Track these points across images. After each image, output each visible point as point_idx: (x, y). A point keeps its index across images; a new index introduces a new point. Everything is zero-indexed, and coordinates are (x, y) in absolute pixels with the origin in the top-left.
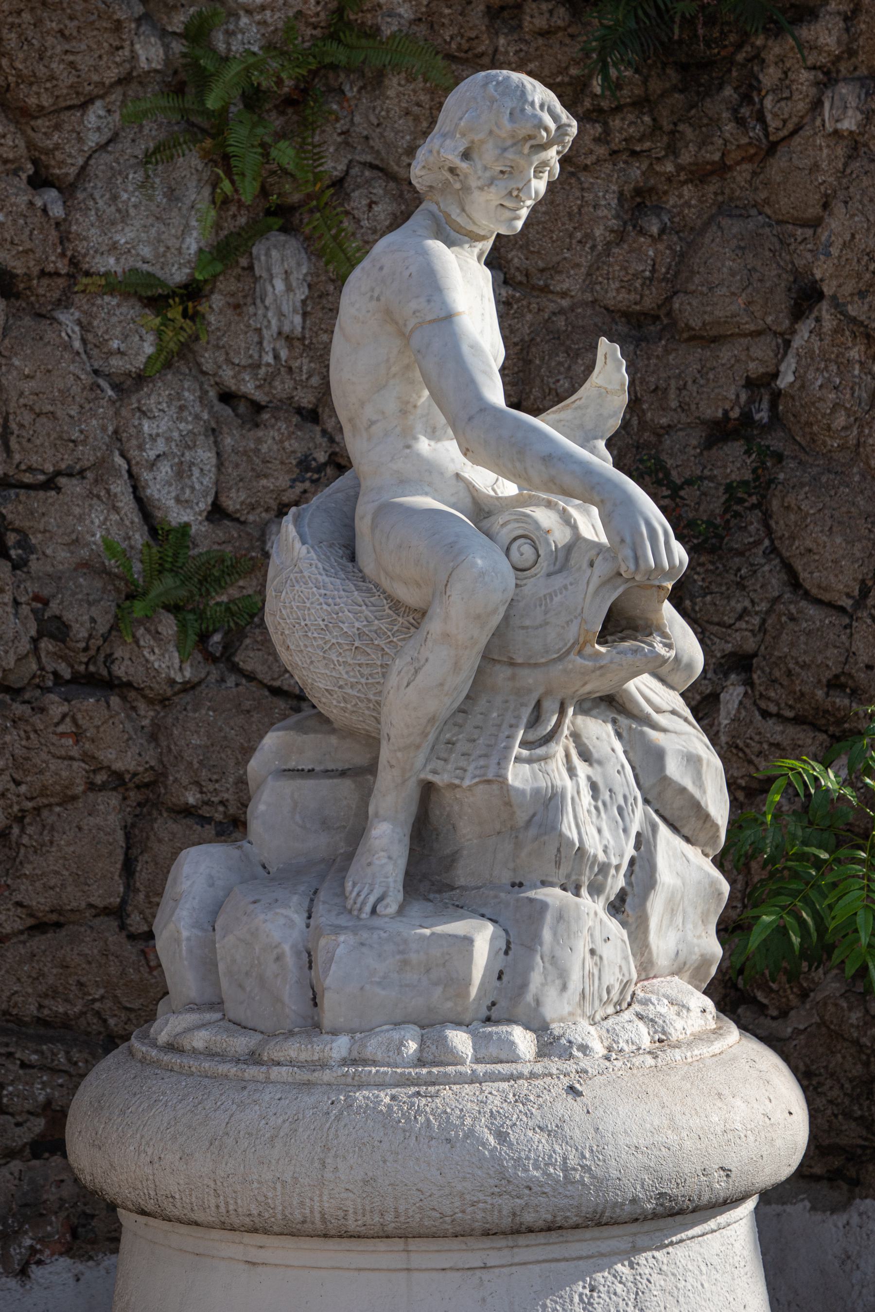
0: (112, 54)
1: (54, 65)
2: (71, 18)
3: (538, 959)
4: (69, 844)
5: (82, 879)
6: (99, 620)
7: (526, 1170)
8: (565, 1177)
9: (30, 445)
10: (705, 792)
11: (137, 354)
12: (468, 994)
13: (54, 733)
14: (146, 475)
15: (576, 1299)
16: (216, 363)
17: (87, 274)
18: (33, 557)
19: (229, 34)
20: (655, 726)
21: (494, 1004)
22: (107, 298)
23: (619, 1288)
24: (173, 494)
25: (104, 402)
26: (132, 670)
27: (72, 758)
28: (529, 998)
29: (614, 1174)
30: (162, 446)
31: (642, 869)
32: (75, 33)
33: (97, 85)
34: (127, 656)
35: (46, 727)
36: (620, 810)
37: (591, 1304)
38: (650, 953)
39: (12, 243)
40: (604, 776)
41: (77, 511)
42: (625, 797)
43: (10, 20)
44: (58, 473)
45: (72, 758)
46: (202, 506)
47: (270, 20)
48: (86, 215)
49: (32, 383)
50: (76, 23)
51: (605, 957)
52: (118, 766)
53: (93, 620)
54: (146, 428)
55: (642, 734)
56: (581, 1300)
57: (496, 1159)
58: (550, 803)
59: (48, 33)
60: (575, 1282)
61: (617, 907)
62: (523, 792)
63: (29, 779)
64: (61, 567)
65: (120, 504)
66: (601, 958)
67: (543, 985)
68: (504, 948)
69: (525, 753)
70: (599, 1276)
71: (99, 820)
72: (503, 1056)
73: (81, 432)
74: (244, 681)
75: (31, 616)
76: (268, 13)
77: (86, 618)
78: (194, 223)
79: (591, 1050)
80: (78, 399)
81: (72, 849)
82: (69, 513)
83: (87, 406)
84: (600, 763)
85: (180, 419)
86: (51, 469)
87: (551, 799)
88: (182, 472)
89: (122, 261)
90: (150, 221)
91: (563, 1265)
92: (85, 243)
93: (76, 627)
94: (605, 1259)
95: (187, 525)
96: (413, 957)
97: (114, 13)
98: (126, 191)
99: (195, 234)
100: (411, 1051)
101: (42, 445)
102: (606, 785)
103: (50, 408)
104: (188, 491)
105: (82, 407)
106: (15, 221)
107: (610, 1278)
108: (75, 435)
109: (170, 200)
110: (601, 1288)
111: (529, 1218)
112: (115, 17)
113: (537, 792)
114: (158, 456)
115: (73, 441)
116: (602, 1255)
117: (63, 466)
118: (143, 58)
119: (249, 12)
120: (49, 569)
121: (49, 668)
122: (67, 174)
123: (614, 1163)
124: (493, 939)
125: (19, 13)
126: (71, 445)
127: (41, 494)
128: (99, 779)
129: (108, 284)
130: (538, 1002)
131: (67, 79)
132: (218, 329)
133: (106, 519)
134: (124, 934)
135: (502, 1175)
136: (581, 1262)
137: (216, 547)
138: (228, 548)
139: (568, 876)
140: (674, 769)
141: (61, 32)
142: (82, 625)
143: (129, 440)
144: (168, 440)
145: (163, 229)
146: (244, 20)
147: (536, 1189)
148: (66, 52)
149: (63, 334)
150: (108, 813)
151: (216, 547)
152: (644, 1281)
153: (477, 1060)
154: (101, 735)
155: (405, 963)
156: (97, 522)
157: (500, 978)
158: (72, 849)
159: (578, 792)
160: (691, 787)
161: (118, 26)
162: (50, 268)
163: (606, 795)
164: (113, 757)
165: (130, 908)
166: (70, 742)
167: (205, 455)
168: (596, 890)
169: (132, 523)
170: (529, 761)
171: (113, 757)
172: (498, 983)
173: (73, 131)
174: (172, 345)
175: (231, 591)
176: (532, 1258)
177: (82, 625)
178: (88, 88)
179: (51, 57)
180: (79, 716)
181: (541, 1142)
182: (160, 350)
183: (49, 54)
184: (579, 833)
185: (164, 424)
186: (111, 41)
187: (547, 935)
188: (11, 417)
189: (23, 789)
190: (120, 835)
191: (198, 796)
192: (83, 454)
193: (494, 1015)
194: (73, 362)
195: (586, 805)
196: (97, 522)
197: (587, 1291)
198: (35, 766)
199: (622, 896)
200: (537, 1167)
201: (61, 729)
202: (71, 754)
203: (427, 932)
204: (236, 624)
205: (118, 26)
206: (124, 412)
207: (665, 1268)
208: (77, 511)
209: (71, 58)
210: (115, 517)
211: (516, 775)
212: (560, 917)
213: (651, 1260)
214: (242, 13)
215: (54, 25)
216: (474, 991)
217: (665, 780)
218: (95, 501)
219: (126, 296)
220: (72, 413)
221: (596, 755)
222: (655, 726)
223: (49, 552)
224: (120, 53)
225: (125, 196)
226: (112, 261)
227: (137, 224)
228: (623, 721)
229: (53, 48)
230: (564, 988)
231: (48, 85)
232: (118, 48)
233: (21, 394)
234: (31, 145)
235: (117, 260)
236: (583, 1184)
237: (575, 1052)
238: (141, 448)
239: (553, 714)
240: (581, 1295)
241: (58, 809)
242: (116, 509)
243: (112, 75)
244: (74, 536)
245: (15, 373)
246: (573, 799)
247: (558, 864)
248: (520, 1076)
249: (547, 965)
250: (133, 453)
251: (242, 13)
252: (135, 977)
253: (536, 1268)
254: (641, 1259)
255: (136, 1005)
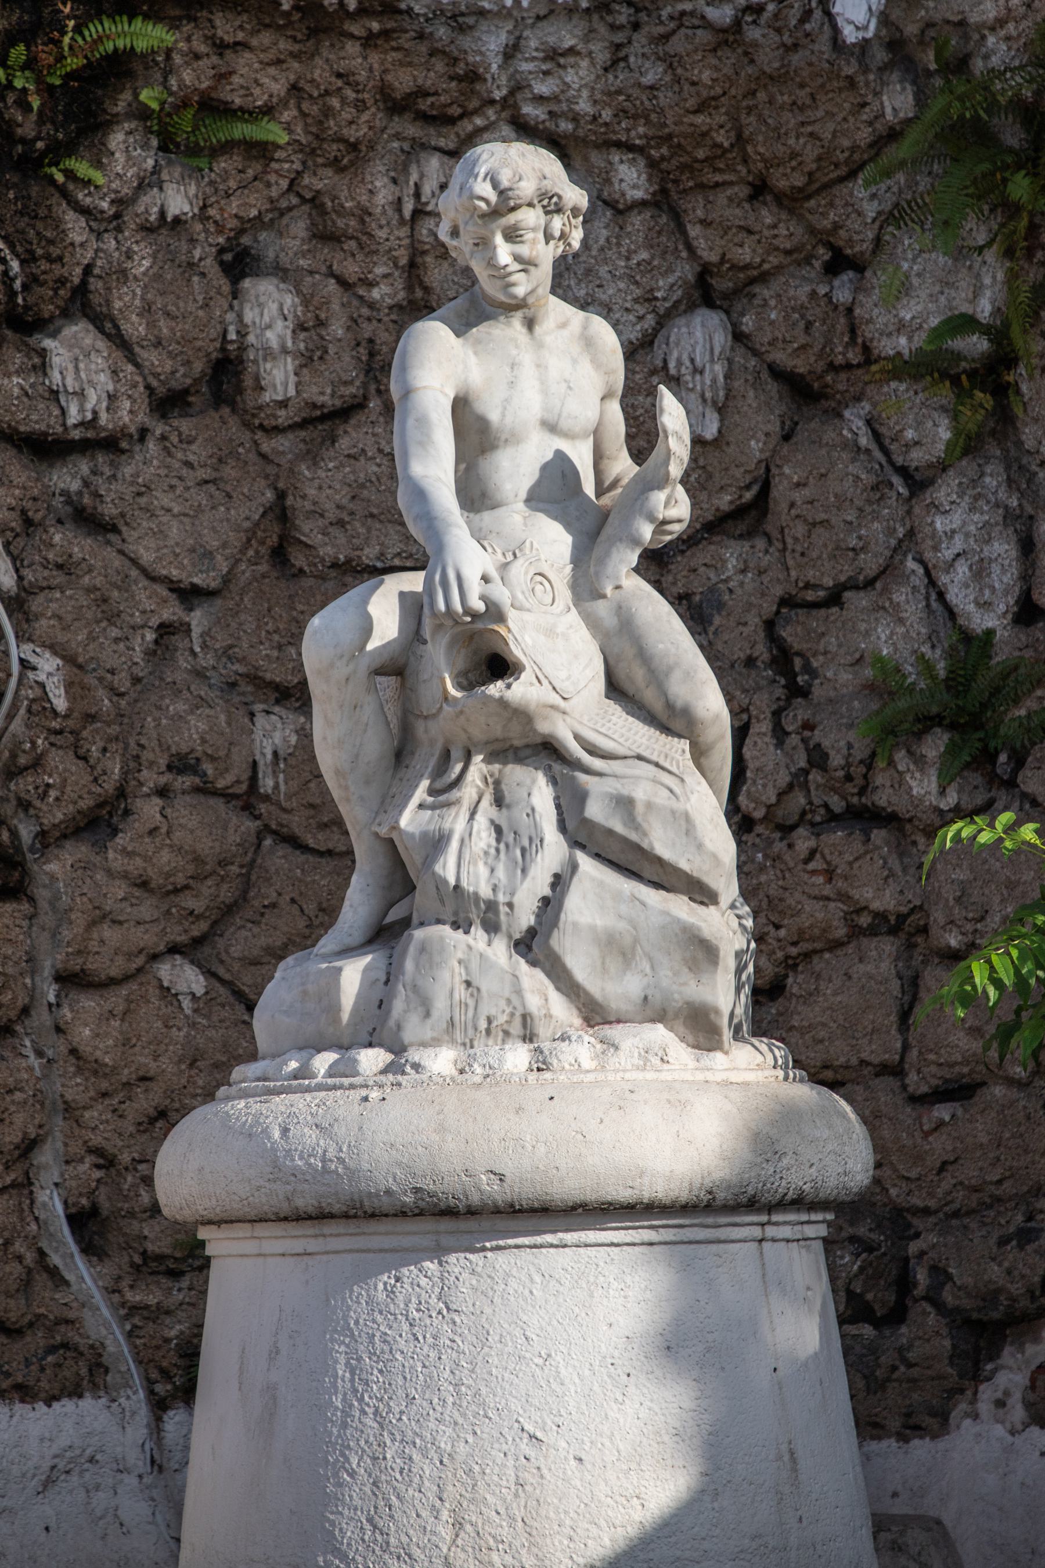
0: (858, 112)
1: (791, 142)
2: (802, 86)
3: (400, 987)
4: (835, 994)
5: (850, 1032)
6: (856, 746)
7: (293, 1160)
8: (323, 1167)
9: (806, 560)
10: (645, 834)
11: (934, 442)
12: (340, 1020)
13: (805, 871)
14: (943, 579)
15: (381, 1286)
16: (1035, 439)
17: (879, 358)
18: (817, 681)
19: (986, 57)
20: (588, 771)
21: (374, 1029)
22: (893, 384)
23: (424, 1281)
24: (972, 597)
25: (893, 501)
26: (894, 799)
27: (828, 899)
28: (391, 1023)
29: (366, 1166)
30: (959, 544)
31: (550, 906)
32: (808, 102)
33: (854, 149)
34: (888, 784)
35: (796, 865)
36: (523, 851)
37: (393, 1292)
38: (584, 990)
39: (784, 341)
40: (509, 819)
41: (863, 626)
42: (531, 839)
43: (744, 104)
44: (844, 587)
45: (828, 899)
46: (1002, 607)
47: (1014, 34)
48: (869, 295)
49: (806, 492)
50: (808, 90)
51: (483, 989)
52: (876, 905)
53: (850, 746)
54: (938, 525)
55: (573, 778)
56: (385, 1288)
57: (274, 1150)
58: (437, 843)
59: (782, 108)
60: (382, 1273)
61: (531, 945)
62: (412, 836)
63: (786, 922)
64: (845, 691)
65: (904, 615)
66: (478, 990)
67: (405, 1012)
68: (384, 978)
69: (430, 799)
70: (405, 1271)
71: (870, 968)
72: (348, 1073)
73: (860, 538)
74: (1027, 806)
75: (801, 746)
76: (1011, 26)
77: (842, 743)
78: (987, 281)
79: (424, 1068)
80: (857, 502)
81: (839, 999)
82: (854, 630)
83: (868, 509)
84: (508, 807)
85: (972, 509)
86: (831, 584)
87: (439, 840)
88: (980, 572)
89: (916, 338)
90: (938, 288)
91: (371, 1255)
92: (871, 326)
93: (832, 753)
94: (413, 1255)
95: (990, 633)
96: (310, 988)
97: (840, 69)
98: (906, 260)
99: (988, 293)
100: (290, 1069)
101: (819, 557)
102: (511, 827)
103: (823, 516)
104: (987, 592)
105: (861, 510)
106: (787, 317)
107: (416, 1271)
108: (853, 542)
109: (956, 260)
110: (405, 1280)
111: (300, 1203)
112: (843, 74)
113: (425, 835)
114: (958, 555)
115: (853, 549)
116: (406, 1250)
117: (843, 578)
118: (888, 110)
119: (993, 29)
120: (832, 694)
121: (817, 801)
122: (862, 253)
123: (366, 1156)
124: (366, 970)
125: (754, 93)
126: (851, 554)
127: (823, 612)
128: (864, 920)
129: (895, 367)
130: (399, 1027)
131: (811, 152)
132: (1031, 399)
133: (892, 633)
134: (905, 1095)
135: (276, 1165)
136: (388, 1255)
137: (1017, 653)
138: (1028, 654)
139: (456, 913)
140: (595, 811)
141: (794, 103)
142: (838, 751)
143: (924, 540)
144: (967, 535)
145: (953, 293)
146: (991, 40)
147: (299, 1176)
148: (803, 124)
149: (845, 432)
150: (881, 958)
151: (1017, 653)
152: (452, 1279)
153: (330, 1074)
154: (855, 871)
155: (305, 993)
156: (883, 637)
157: (380, 1007)
158: (839, 999)
159: (470, 835)
160: (619, 828)
161: (851, 82)
162: (839, 360)
163: (510, 838)
164: (870, 895)
165: (907, 1066)
166: (821, 880)
167: (1003, 549)
168: (491, 927)
169: (918, 634)
170: (433, 807)
171: (870, 895)
172: (378, 1012)
173: (847, 204)
174: (970, 426)
175: (1028, 703)
176: (340, 1247)
177: (838, 751)
178: (842, 157)
179: (786, 134)
180: (826, 851)
181: (311, 1136)
182: (957, 432)
183: (783, 131)
184: (458, 873)
185: (956, 519)
186: (852, 100)
187: (409, 965)
188: (786, 531)
189: (782, 933)
190: (895, 986)
191: (960, 937)
192: (865, 562)
193: (374, 1040)
194: (854, 460)
195: (482, 845)
196: (883, 637)
197: (393, 1282)
198: (789, 907)
199: (532, 932)
200: (301, 1158)
201: (811, 866)
202: (825, 893)
203: (324, 966)
204: (1030, 739)
205: (851, 82)
206: (917, 510)
207: (479, 1269)
208: (863, 626)
209: (809, 129)
210: (900, 630)
211: (412, 821)
212: (423, 949)
213: (462, 1261)
214: (986, 32)
215: (786, 97)
216: (345, 1016)
217: (586, 823)
218: (881, 612)
219: (916, 378)
220: (849, 518)
221: (507, 800)
222: (588, 771)
223: (829, 674)
224: (867, 110)
225: (905, 266)
226: (903, 341)
227: (923, 295)
228: (557, 767)
229: (788, 122)
230: (427, 1014)
231: (794, 163)
232: (864, 105)
233: (792, 505)
234: (812, 231)
235: (910, 339)
236: (338, 1174)
237: (408, 1069)
238: (936, 548)
239: (457, 761)
240: (385, 1284)
241: (827, 955)
242: (901, 621)
243: (864, 136)
244: (857, 656)
245: (785, 482)
246: (462, 841)
247: (442, 901)
248: (341, 1087)
249: (410, 993)
250: (928, 555)
251: (986, 32)
252: (909, 1143)
253: (349, 1257)
254: (452, 1258)
255: (913, 1174)
